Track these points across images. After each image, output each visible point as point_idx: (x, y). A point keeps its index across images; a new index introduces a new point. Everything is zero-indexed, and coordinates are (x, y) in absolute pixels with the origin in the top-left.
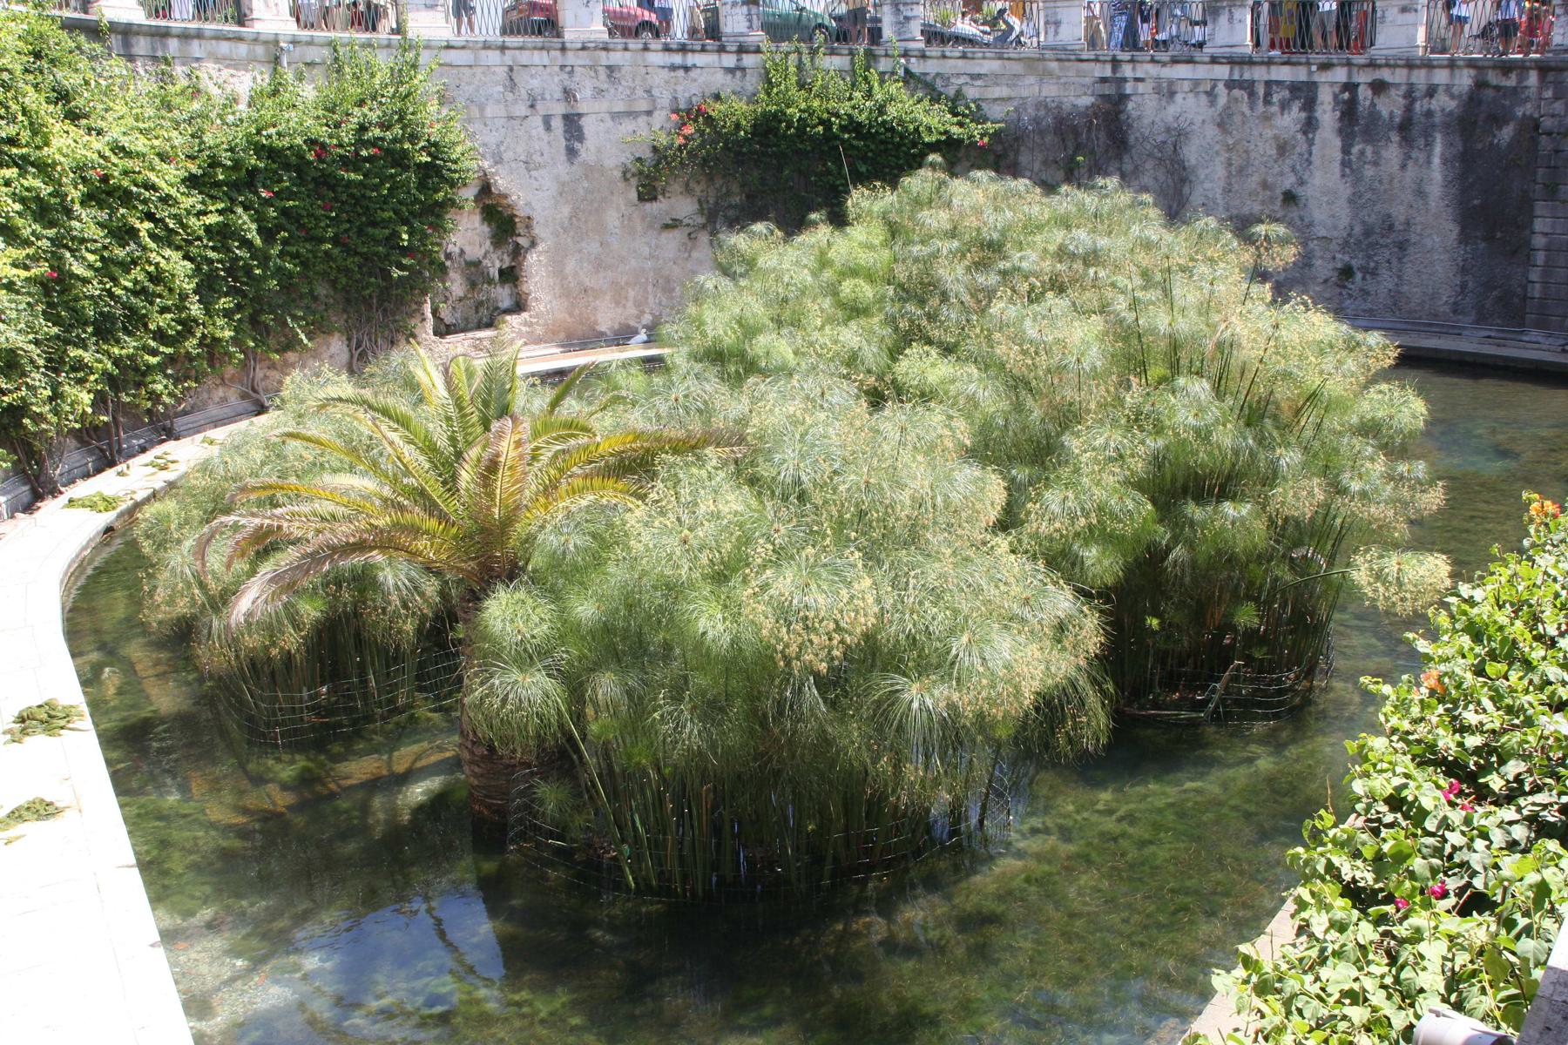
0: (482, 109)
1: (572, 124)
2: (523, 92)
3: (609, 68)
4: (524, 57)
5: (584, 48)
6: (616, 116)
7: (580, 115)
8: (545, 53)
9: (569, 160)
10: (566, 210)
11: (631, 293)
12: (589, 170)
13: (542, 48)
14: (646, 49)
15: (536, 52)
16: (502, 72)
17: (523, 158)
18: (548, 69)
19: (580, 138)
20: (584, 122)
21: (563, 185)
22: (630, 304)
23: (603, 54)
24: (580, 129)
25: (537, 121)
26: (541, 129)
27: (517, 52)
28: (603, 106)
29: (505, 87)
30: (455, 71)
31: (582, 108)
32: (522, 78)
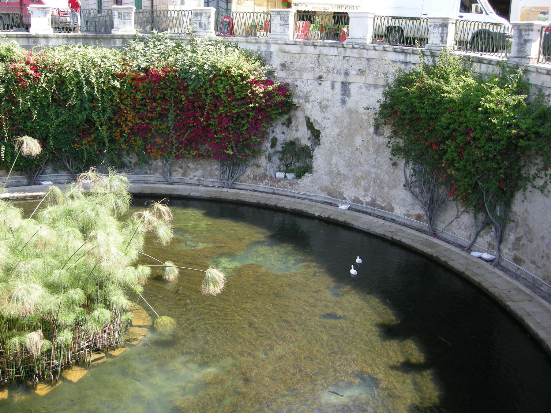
1: (345, 85)
2: (324, 67)
3: (368, 59)
4: (325, 50)
5: (354, 48)
6: (368, 86)
7: (350, 83)
8: (336, 49)
9: (342, 105)
11: (363, 183)
12: (350, 112)
13: (334, 47)
14: (385, 50)
15: (332, 48)
16: (315, 57)
17: (319, 101)
18: (337, 57)
21: (337, 117)
22: (362, 188)
23: (365, 51)
26: (330, 88)
27: (322, 48)
28: (361, 79)
29: (315, 65)
30: (291, 55)
31: (351, 79)
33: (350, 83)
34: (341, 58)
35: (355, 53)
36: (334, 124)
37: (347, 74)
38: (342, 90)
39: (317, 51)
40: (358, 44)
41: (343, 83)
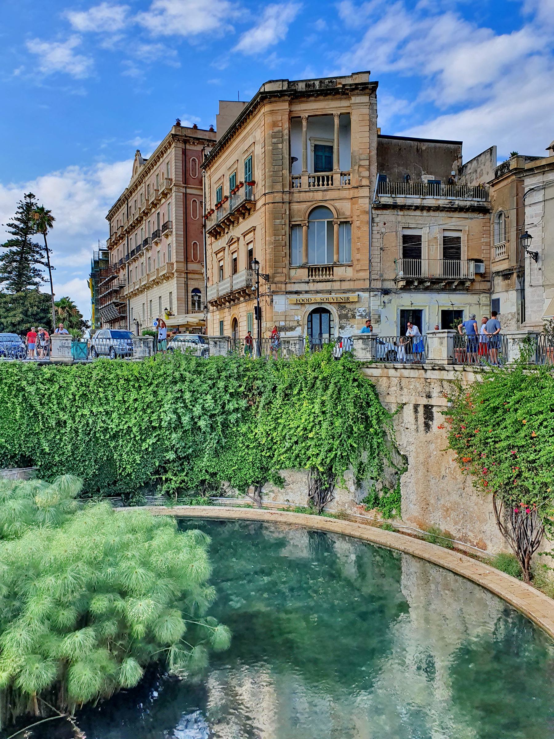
1: (428, 409)
4: (406, 373)
7: (432, 406)
9: (425, 430)
19: (431, 419)
24: (432, 413)
31: (433, 402)
34: (423, 380)
35: (436, 375)
37: (429, 396)
38: (424, 414)
39: (398, 374)
40: (438, 365)
41: (426, 406)
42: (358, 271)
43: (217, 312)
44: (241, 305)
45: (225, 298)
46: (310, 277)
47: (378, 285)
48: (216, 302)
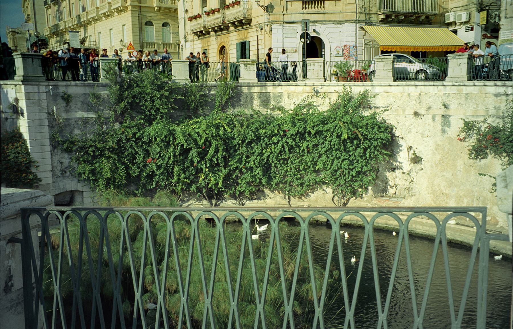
0: (404, 111)
2: (424, 104)
7: (449, 116)
9: (442, 135)
10: (438, 157)
19: (449, 126)
20: (451, 119)
24: (449, 122)
25: (430, 117)
29: (416, 102)
32: (424, 97)
33: (449, 116)
36: (435, 151)
42: (346, 5)
43: (199, 41)
44: (231, 35)
45: (214, 28)
46: (304, 9)
47: (363, 17)
48: (201, 32)
